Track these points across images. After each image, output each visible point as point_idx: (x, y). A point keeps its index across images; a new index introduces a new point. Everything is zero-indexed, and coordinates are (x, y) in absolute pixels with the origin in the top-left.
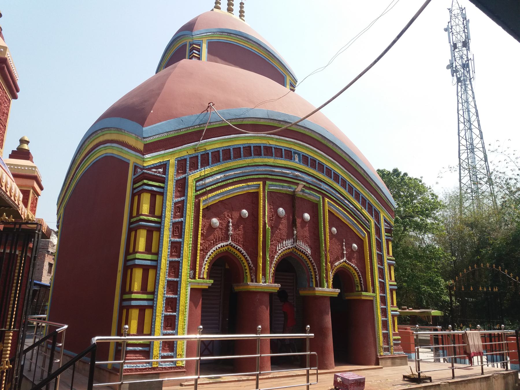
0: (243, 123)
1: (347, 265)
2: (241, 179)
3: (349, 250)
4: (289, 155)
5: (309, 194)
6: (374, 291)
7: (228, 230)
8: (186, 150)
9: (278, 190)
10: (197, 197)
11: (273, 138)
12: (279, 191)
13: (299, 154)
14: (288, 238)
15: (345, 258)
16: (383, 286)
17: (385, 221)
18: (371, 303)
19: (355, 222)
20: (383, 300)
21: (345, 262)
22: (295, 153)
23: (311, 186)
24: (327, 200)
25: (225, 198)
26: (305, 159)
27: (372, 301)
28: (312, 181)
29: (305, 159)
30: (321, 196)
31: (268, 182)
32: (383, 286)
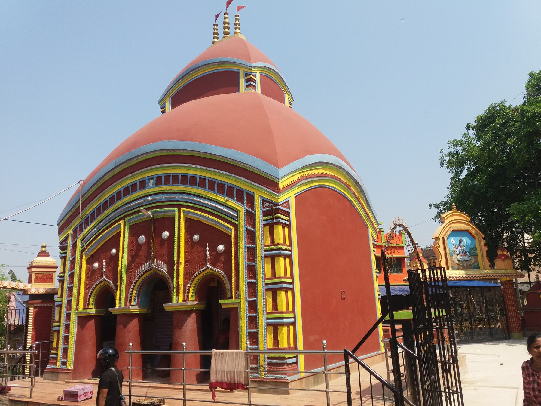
0: (105, 180)
1: (212, 272)
2: (107, 226)
3: (214, 254)
4: (143, 184)
5: (164, 212)
6: (238, 297)
7: (102, 269)
8: (76, 223)
9: (136, 221)
10: (82, 252)
11: (128, 178)
12: (140, 221)
13: (153, 179)
14: (147, 261)
15: (208, 265)
16: (252, 288)
17: (264, 201)
18: (236, 311)
19: (217, 220)
20: (253, 306)
21: (208, 268)
22: (149, 180)
23: (165, 203)
24: (182, 209)
25: (101, 244)
26: (159, 180)
27: (237, 308)
28: (165, 198)
29: (159, 180)
30: (176, 210)
31: (126, 219)
32: (252, 288)
